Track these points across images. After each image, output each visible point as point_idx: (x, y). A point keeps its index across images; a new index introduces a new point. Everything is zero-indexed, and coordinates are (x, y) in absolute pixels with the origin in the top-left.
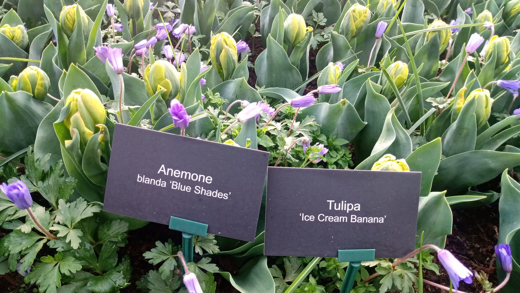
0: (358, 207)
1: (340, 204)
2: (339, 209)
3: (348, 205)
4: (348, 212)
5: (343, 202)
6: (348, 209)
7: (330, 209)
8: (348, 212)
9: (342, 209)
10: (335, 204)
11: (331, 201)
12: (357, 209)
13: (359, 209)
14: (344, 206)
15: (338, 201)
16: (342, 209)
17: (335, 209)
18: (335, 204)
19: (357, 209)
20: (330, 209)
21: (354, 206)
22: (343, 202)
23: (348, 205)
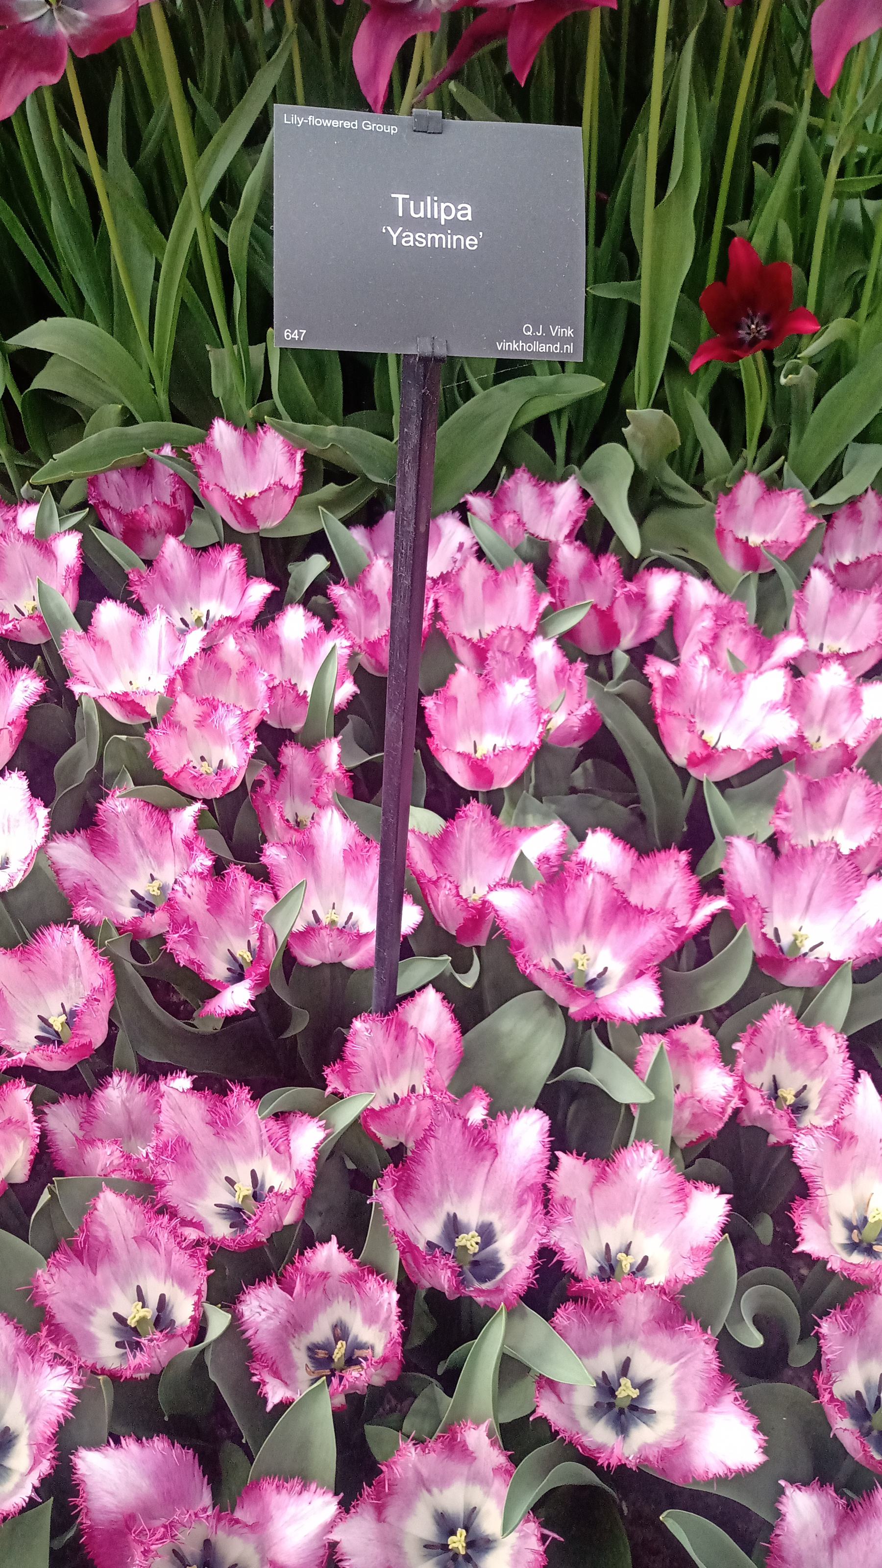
0: (465, 213)
1: (422, 203)
2: (422, 215)
3: (443, 206)
4: (443, 223)
5: (429, 198)
6: (443, 217)
7: (400, 214)
8: (443, 223)
9: (429, 216)
10: (412, 203)
11: (401, 197)
12: (463, 216)
13: (469, 218)
14: (433, 208)
15: (418, 197)
16: (429, 216)
18: (412, 203)
20: (400, 214)
21: (457, 210)
22: (429, 198)
23: (443, 206)
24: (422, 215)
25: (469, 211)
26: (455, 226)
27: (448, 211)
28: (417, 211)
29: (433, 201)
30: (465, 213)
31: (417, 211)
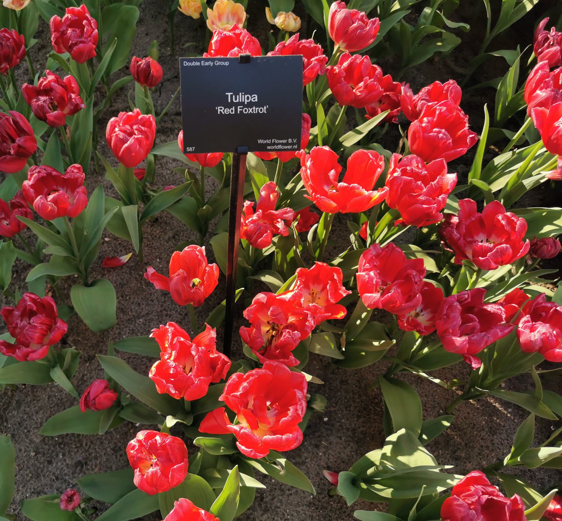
0: (255, 98)
2: (238, 101)
3: (246, 96)
5: (240, 94)
6: (246, 101)
7: (229, 101)
10: (234, 96)
11: (229, 94)
12: (254, 99)
13: (256, 100)
15: (236, 94)
17: (234, 101)
18: (234, 96)
19: (254, 99)
20: (229, 101)
23: (246, 96)
24: (238, 101)
25: (256, 98)
26: (250, 105)
27: (248, 98)
28: (236, 99)
29: (242, 95)
30: (255, 98)
31: (236, 99)
